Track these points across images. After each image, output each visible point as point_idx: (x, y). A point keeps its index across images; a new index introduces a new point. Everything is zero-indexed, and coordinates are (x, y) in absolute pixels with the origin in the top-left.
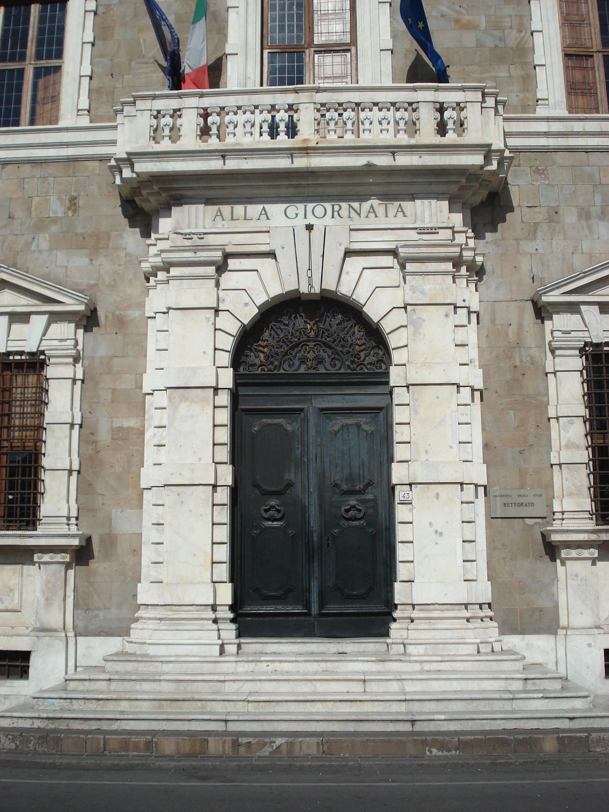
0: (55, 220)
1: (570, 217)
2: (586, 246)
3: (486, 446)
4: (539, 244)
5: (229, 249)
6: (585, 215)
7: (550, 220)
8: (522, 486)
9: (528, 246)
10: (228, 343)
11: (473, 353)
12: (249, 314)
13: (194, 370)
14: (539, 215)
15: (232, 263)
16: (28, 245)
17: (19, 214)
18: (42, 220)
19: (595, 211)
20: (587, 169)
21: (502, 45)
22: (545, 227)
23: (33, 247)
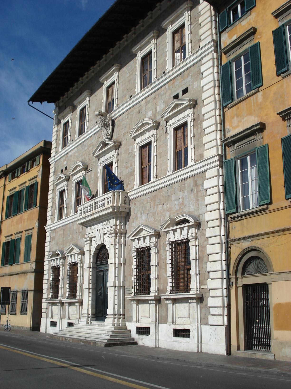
0: (80, 232)
5: (91, 237)
15: (93, 239)
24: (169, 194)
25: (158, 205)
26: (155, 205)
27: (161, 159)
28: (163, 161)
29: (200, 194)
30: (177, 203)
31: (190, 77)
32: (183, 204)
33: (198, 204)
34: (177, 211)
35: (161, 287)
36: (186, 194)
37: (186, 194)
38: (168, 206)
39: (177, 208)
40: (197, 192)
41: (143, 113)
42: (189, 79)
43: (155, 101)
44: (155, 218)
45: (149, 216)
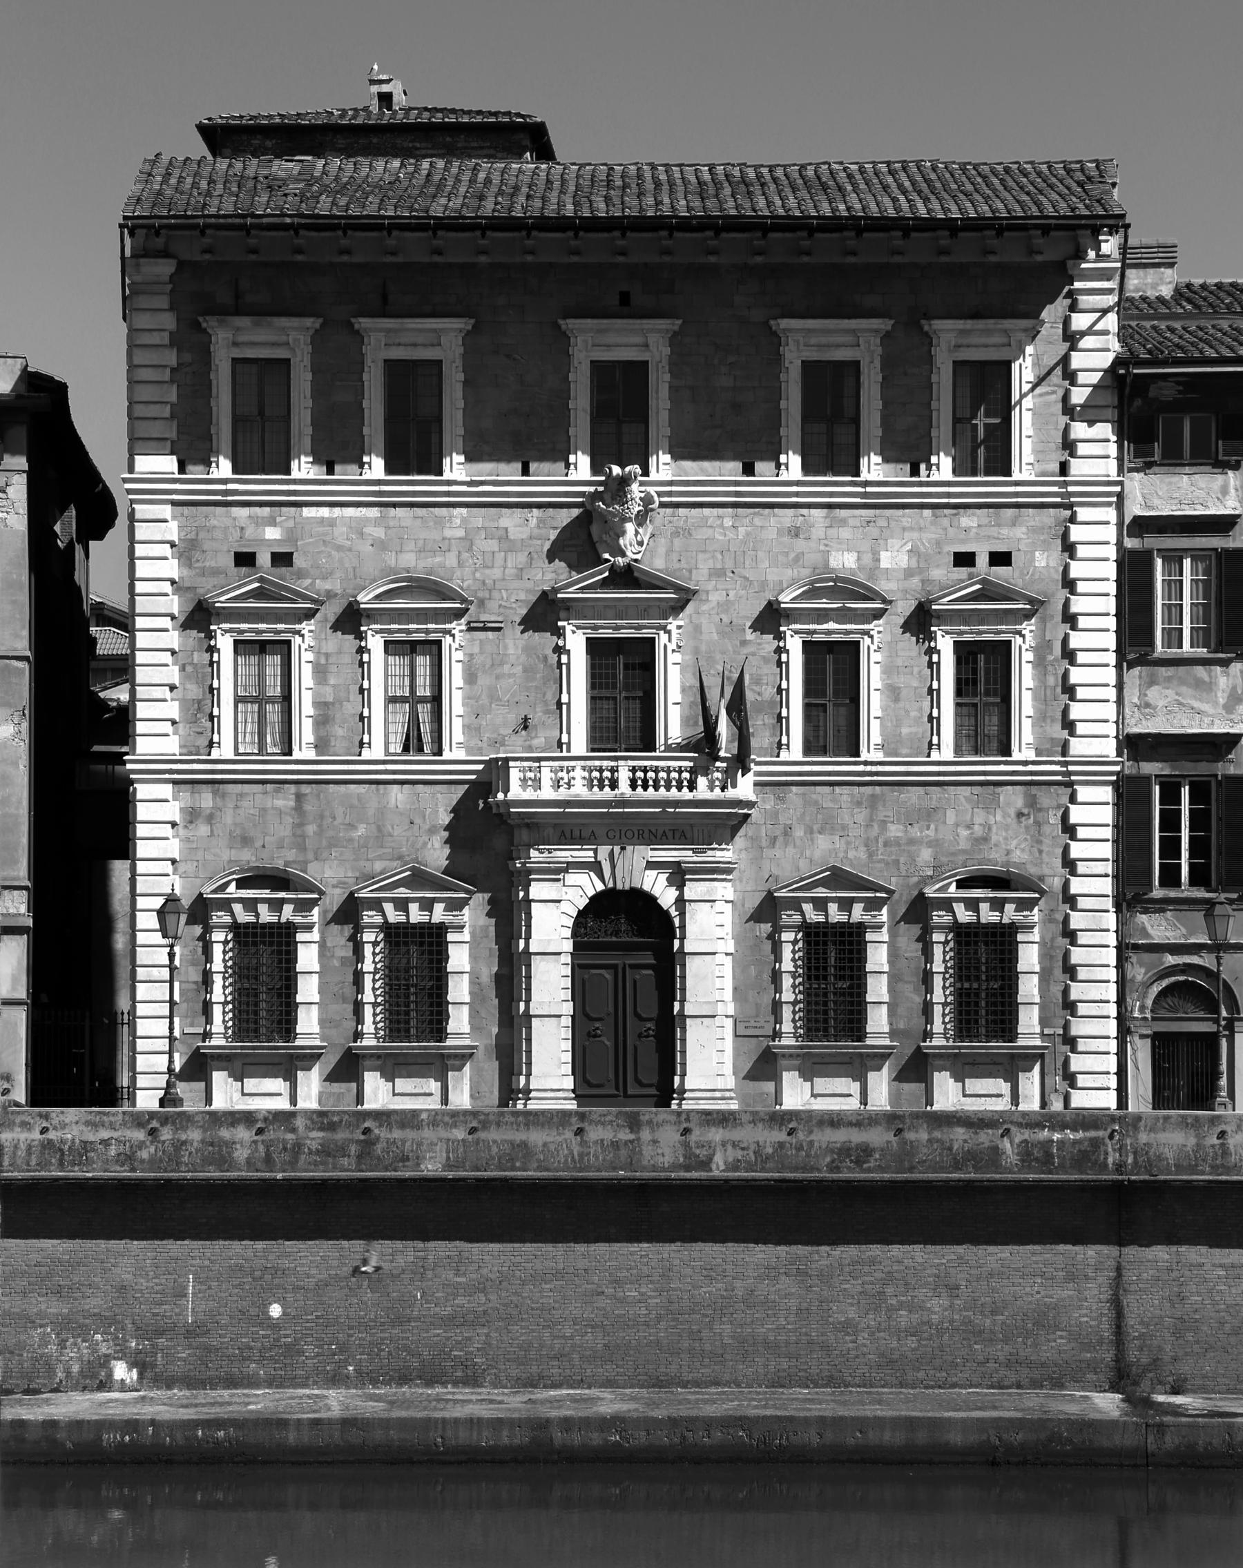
1: (799, 832)
2: (808, 853)
3: (735, 989)
4: (778, 852)
6: (810, 831)
7: (786, 834)
8: (757, 1016)
9: (768, 853)
10: (570, 923)
11: (728, 928)
12: (582, 903)
13: (549, 941)
14: (778, 831)
16: (425, 844)
17: (417, 821)
18: (434, 826)
19: (815, 828)
20: (814, 796)
21: (759, 699)
22: (781, 839)
23: (429, 846)
24: (934, 804)
25: (885, 823)
26: (872, 820)
27: (901, 704)
28: (907, 712)
29: (1046, 829)
30: (964, 833)
31: (1024, 529)
32: (986, 839)
33: (1040, 852)
34: (964, 852)
35: (901, 1026)
36: (998, 818)
37: (998, 818)
38: (931, 833)
39: (964, 845)
40: (1038, 824)
41: (812, 544)
42: (1020, 532)
43: (873, 531)
44: (870, 855)
45: (848, 843)
